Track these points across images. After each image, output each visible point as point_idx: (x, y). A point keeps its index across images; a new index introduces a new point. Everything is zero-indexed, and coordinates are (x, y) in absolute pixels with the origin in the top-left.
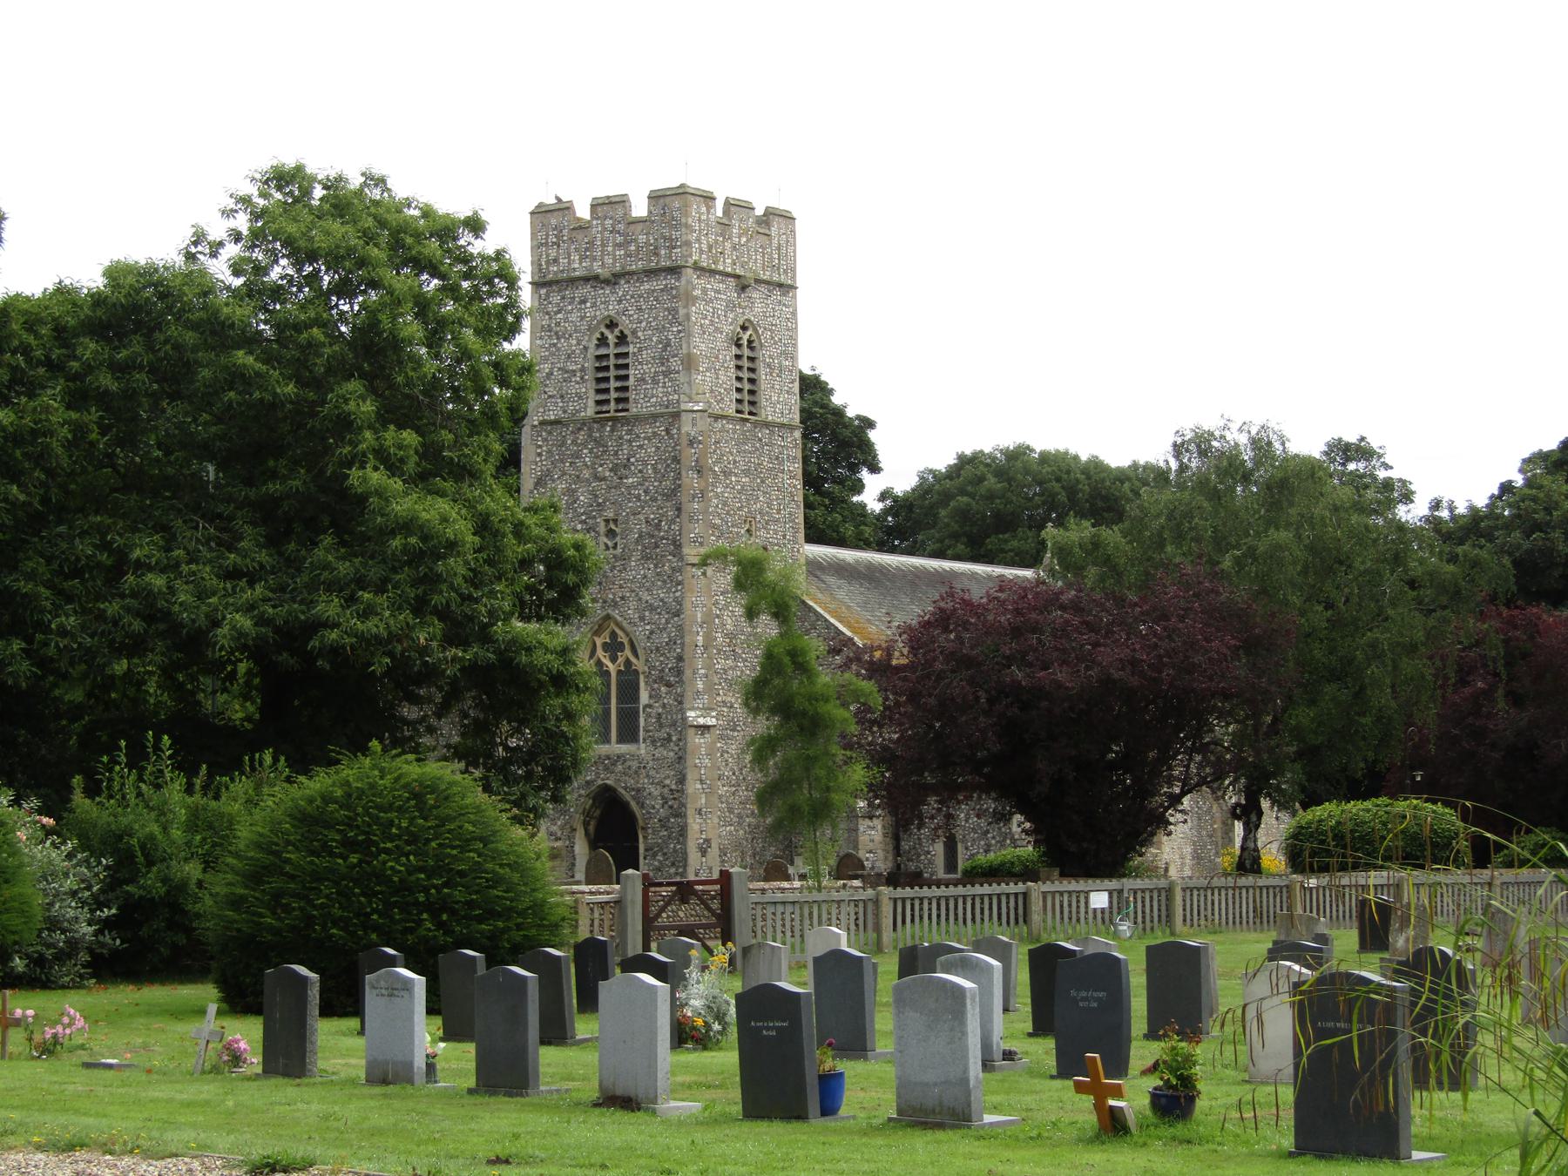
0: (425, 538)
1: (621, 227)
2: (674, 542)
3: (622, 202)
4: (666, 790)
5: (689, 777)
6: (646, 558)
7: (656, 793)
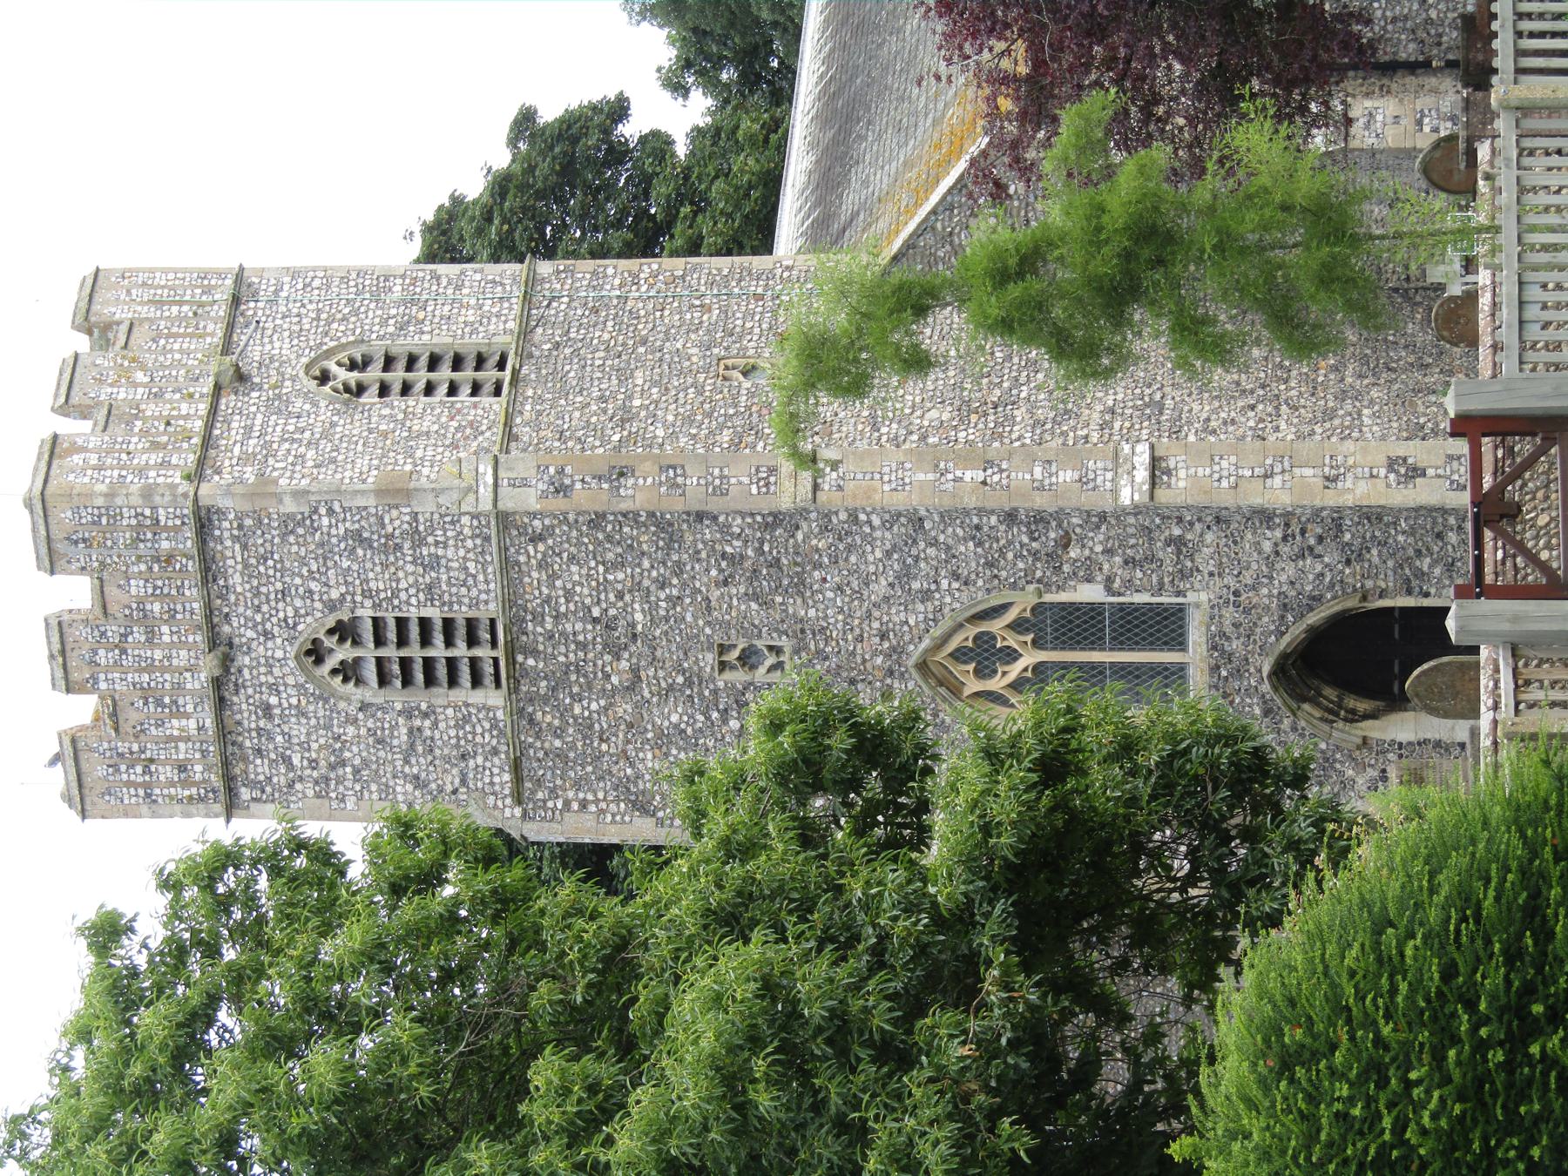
0: (755, 1041)
1: (113, 631)
2: (766, 526)
3: (60, 628)
4: (1285, 549)
5: (1257, 501)
6: (800, 586)
7: (1291, 570)
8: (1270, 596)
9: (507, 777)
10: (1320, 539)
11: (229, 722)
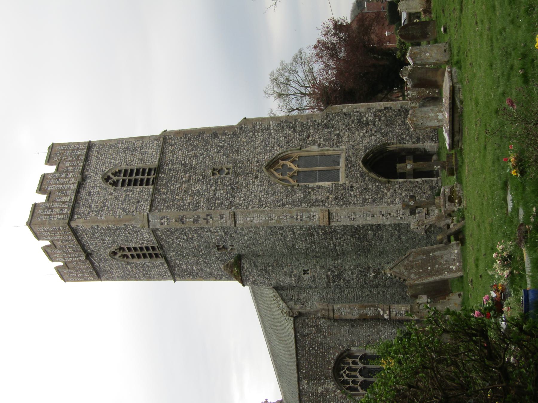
4: (366, 135)
8: (362, 146)
9: (148, 207)
10: (376, 132)
11: (78, 197)
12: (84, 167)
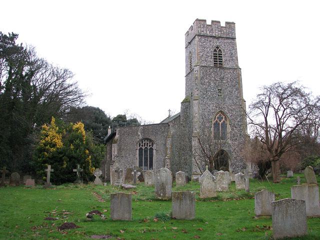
1: (220, 27)
12: (224, 37)
